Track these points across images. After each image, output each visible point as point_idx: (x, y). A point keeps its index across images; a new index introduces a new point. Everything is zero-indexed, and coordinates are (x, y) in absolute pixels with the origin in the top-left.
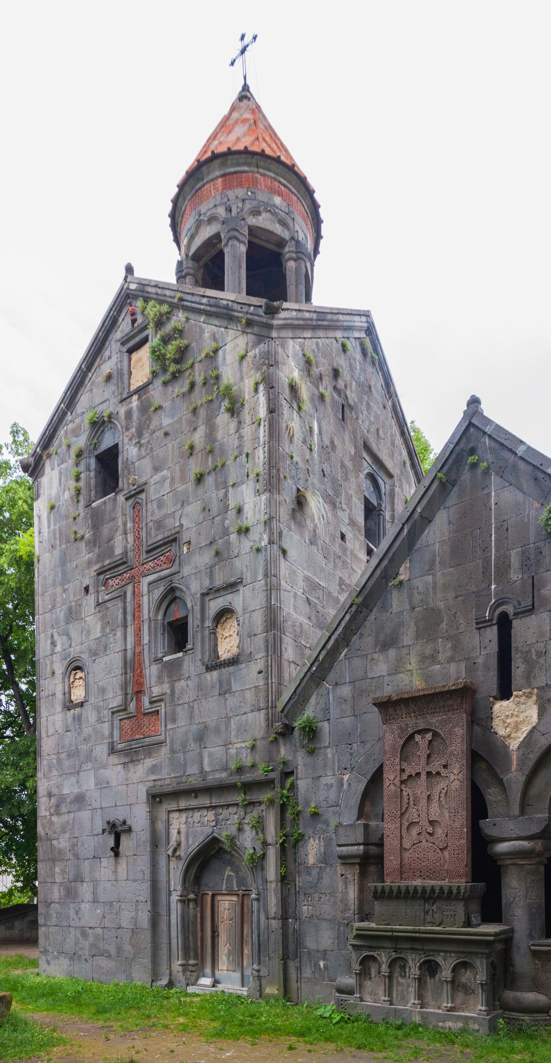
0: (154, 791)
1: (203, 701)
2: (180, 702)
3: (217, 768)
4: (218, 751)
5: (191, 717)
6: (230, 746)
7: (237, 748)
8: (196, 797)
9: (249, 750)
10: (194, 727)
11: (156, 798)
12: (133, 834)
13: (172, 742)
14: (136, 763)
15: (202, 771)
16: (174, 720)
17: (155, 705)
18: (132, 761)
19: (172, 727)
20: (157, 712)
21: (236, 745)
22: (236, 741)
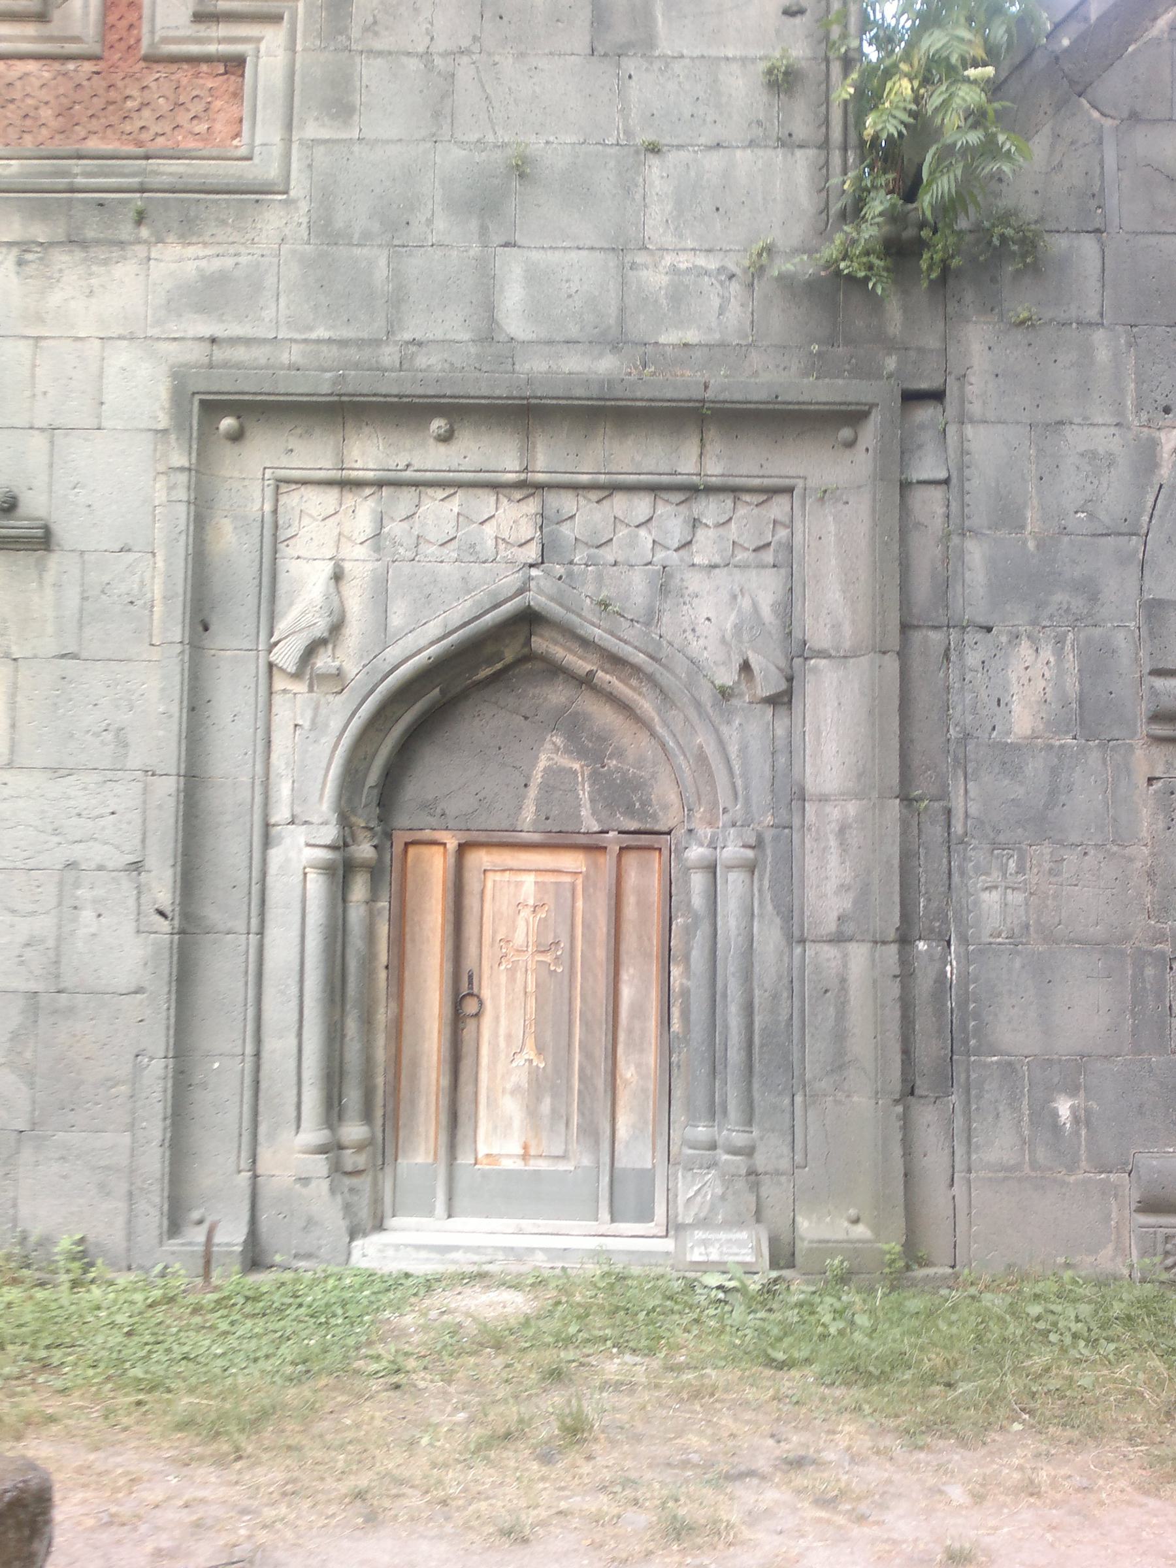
0: (224, 385)
1: (507, 64)
2: (378, 45)
3: (573, 331)
4: (580, 272)
5: (440, 108)
6: (641, 258)
7: (674, 270)
8: (446, 438)
9: (735, 287)
10: (450, 158)
11: (221, 412)
12: (54, 561)
13: (325, 197)
14: (101, 253)
15: (489, 333)
16: (340, 105)
17: (223, 30)
18: (74, 241)
19: (325, 134)
20: (235, 64)
21: (668, 259)
22: (669, 240)
